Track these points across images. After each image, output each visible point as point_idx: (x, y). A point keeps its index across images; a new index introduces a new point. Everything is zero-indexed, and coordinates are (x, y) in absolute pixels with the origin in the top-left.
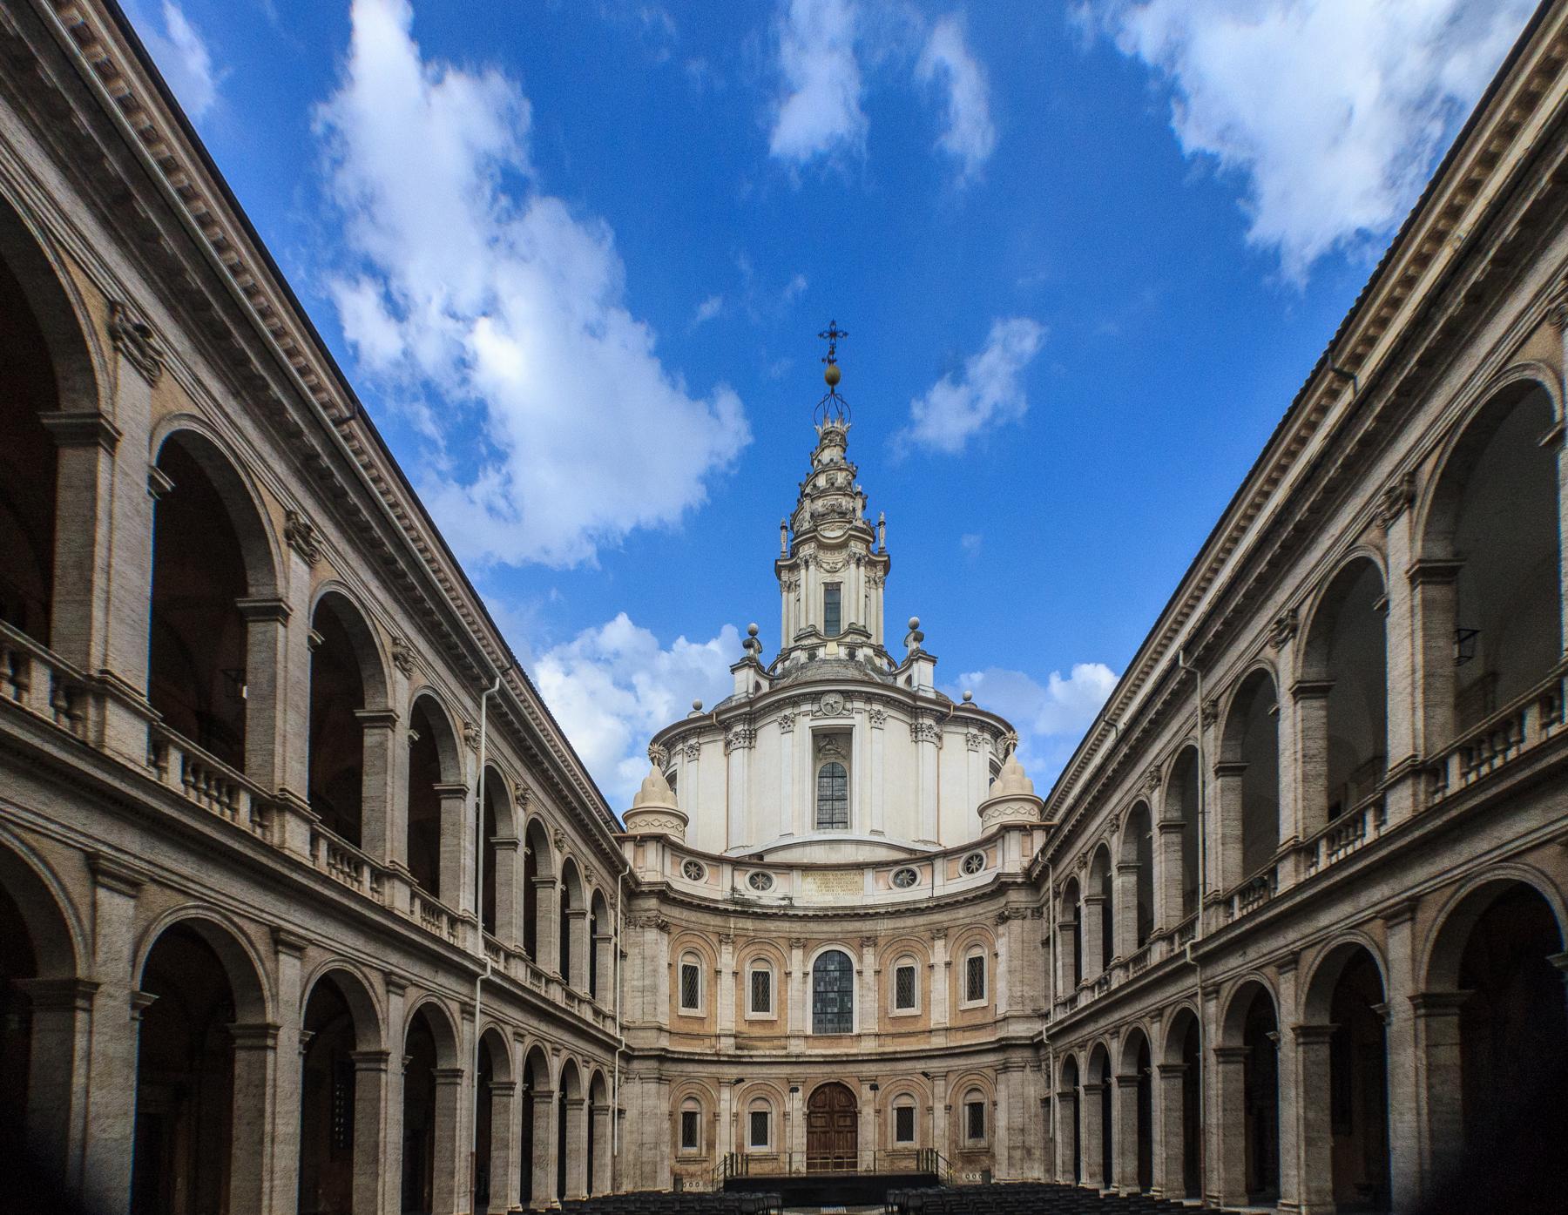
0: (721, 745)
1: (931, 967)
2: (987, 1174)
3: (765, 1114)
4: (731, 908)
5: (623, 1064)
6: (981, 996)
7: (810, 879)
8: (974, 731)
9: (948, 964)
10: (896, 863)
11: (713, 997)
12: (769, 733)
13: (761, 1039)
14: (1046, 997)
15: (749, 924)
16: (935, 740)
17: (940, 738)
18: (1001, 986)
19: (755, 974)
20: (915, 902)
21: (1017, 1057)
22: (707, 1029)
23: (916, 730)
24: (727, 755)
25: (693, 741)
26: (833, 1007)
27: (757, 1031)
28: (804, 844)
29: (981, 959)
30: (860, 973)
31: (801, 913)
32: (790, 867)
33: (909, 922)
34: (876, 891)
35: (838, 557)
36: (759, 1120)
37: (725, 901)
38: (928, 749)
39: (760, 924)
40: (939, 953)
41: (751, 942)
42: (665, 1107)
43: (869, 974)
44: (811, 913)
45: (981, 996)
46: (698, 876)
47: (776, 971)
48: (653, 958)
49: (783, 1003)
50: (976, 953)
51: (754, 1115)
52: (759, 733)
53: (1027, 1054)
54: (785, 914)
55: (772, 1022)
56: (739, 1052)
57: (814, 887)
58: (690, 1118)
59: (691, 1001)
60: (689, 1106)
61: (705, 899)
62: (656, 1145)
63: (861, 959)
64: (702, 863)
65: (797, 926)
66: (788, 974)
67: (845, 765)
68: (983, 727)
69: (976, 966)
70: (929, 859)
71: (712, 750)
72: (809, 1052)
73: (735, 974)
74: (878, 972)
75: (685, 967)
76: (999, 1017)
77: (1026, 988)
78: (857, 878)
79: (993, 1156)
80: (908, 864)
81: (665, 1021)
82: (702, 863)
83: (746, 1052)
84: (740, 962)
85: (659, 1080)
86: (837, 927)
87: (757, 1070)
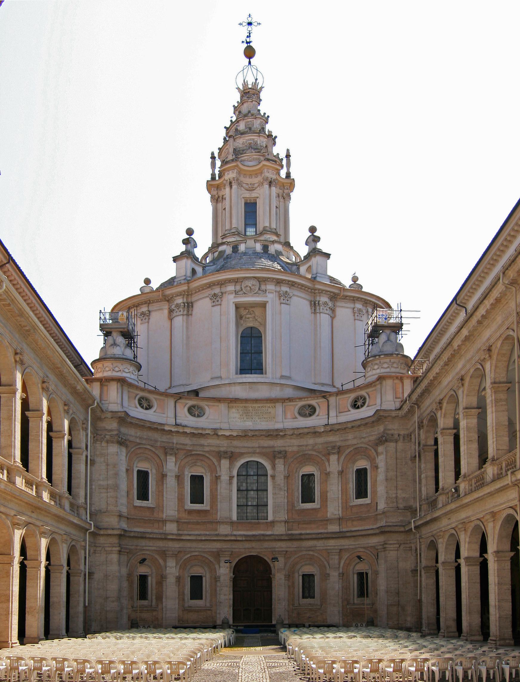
11: (160, 493)
14: (415, 498)
19: (192, 477)
20: (314, 427)
26: (252, 506)
29: (365, 470)
31: (227, 433)
33: (311, 441)
34: (285, 419)
39: (195, 441)
44: (235, 434)
59: (143, 494)
63: (274, 467)
66: (218, 478)
77: (399, 492)
80: (309, 399)
86: (254, 444)
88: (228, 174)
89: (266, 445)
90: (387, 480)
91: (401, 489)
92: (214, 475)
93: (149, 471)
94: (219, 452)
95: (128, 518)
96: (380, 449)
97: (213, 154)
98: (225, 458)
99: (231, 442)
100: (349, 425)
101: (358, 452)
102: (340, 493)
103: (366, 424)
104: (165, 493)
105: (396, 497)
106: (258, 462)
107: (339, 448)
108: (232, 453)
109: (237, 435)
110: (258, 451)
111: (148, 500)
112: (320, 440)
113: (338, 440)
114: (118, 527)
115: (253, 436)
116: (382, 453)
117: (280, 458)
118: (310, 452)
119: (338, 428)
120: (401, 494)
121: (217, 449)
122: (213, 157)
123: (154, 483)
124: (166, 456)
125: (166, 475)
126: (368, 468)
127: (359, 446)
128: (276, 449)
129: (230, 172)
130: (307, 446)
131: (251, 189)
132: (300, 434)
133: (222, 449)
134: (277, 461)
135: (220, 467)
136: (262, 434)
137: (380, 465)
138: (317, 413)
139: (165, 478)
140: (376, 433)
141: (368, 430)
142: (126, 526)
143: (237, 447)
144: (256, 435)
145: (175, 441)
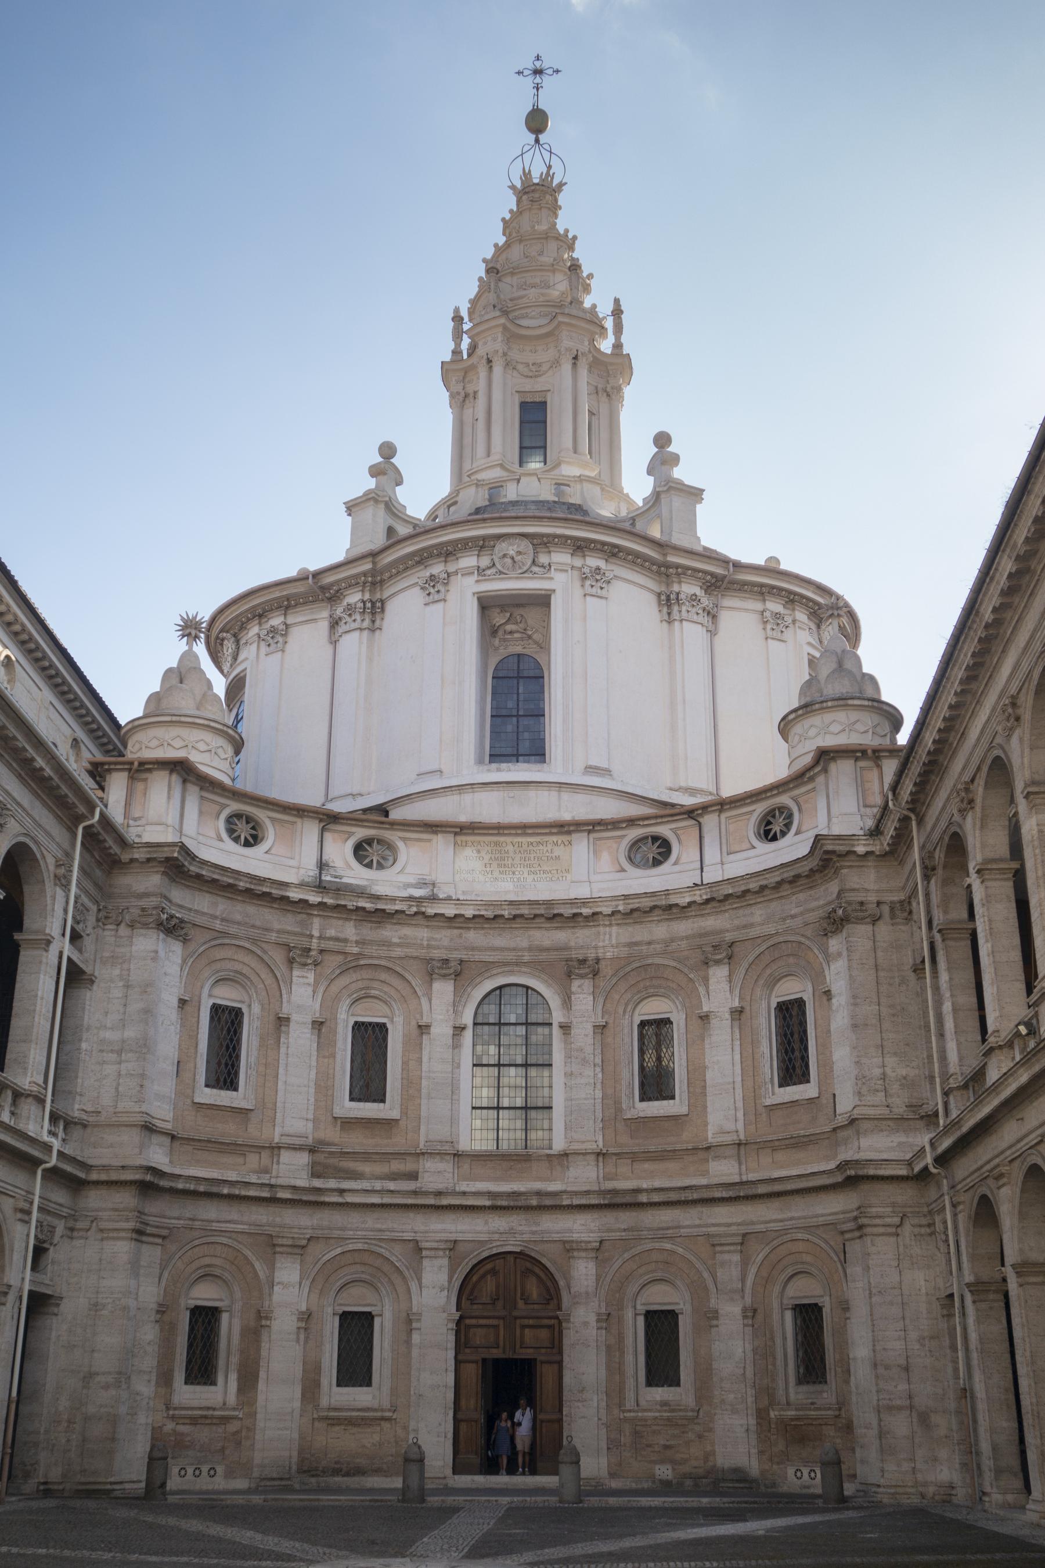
0: (324, 625)
1: (705, 1018)
2: (834, 1466)
3: (369, 1317)
4: (314, 898)
5: (60, 1196)
6: (805, 1078)
7: (469, 852)
8: (774, 606)
9: (738, 1013)
10: (632, 822)
11: (270, 1070)
12: (406, 604)
13: (366, 1157)
15: (349, 930)
16: (705, 619)
17: (714, 617)
18: (842, 1055)
19: (358, 1026)
20: (667, 893)
21: (883, 1202)
22: (254, 1132)
23: (668, 602)
24: (334, 643)
25: (276, 621)
27: (357, 1141)
28: (460, 788)
29: (800, 1003)
30: (565, 1028)
31: (450, 911)
32: (433, 827)
33: (659, 930)
34: (593, 874)
35: (544, 355)
36: (356, 1327)
37: (302, 885)
39: (368, 932)
40: (719, 992)
41: (352, 964)
42: (150, 1293)
43: (583, 1033)
44: (469, 912)
45: (805, 1078)
46: (253, 840)
47: (399, 1020)
48: (147, 987)
49: (411, 1085)
50: (789, 989)
51: (345, 1317)
52: (390, 607)
53: (904, 1195)
54: (418, 912)
55: (387, 1125)
56: (317, 1183)
57: (477, 865)
58: (205, 1319)
59: (225, 1072)
60: (205, 1294)
61: (262, 880)
62: (123, 1377)
63: (567, 1002)
64: (262, 815)
65: (444, 937)
66: (423, 1029)
67: (541, 659)
68: (792, 599)
69: (791, 1018)
70: (692, 813)
71: (308, 634)
72: (463, 1187)
73: (318, 1025)
74: (601, 1029)
75: (216, 1009)
76: (841, 1120)
78: (558, 851)
79: (849, 1428)
81: (163, 1113)
82: (262, 815)
83: (332, 1184)
84: (330, 1004)
85: (139, 1234)
86: (520, 939)
87: (353, 1220)
88: (485, 343)
89: (547, 943)
90: (855, 1026)
91: (895, 1054)
92: (414, 1023)
93: (245, 1010)
94: (429, 961)
95: (173, 1137)
96: (835, 944)
97: (457, 310)
98: (444, 976)
99: (460, 936)
100: (753, 885)
101: (781, 954)
102: (738, 1068)
103: (797, 877)
104: (281, 1071)
105: (884, 1074)
106: (527, 988)
107: (731, 945)
108: (461, 962)
109: (475, 916)
110: (526, 959)
111: (236, 1089)
112: (683, 927)
114: (139, 1162)
115: (515, 917)
116: (839, 954)
117: (582, 977)
118: (658, 961)
120: (896, 1068)
121: (422, 953)
122: (457, 319)
123: (255, 1043)
124: (291, 969)
125: (288, 1019)
126: (807, 997)
127: (781, 939)
128: (574, 955)
129: (489, 339)
130: (649, 943)
131: (536, 371)
132: (632, 911)
133: (437, 954)
134: (575, 984)
135: (430, 1000)
136: (538, 912)
137: (834, 990)
139: (283, 1028)
140: (822, 902)
141: (802, 896)
142: (167, 1160)
143: (473, 949)
144: (521, 916)
145: (316, 933)
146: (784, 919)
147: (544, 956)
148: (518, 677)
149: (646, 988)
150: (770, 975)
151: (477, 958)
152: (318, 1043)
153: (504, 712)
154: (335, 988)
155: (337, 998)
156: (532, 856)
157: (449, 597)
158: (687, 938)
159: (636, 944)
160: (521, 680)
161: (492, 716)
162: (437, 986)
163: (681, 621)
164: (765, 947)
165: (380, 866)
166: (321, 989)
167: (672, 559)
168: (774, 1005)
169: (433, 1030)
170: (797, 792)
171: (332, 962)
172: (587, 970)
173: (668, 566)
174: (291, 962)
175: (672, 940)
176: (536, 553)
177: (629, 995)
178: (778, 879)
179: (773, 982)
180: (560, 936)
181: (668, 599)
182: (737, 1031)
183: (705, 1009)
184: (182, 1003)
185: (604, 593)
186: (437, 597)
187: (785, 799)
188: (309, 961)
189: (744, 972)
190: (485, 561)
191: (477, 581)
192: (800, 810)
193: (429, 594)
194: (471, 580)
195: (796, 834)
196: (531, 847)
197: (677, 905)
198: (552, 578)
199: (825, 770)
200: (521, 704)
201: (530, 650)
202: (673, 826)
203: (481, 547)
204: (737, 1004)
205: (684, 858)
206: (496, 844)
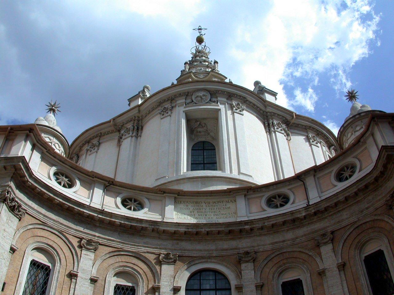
1: (322, 274)
9: (342, 267)
25: (95, 141)
29: (380, 253)
38: (281, 137)
40: (329, 258)
50: (371, 249)
63: (239, 275)
73: (93, 281)
75: (34, 264)
89: (225, 246)
100: (341, 198)
103: (366, 187)
106: (216, 272)
107: (332, 233)
109: (185, 233)
110: (214, 255)
113: (328, 224)
117: (247, 262)
119: (326, 206)
125: (76, 276)
127: (361, 222)
130: (284, 241)
132: (273, 225)
134: (243, 266)
138: (291, 201)
141: (370, 198)
143: (185, 250)
146: (362, 211)
147: (224, 253)
148: (204, 150)
149: (284, 264)
150: (358, 243)
151: (187, 254)
152: (94, 292)
153: (197, 162)
154: (105, 264)
155: (107, 269)
156: (215, 208)
157: (173, 115)
158: (305, 235)
159: (276, 243)
160: (205, 151)
161: (192, 164)
162: (164, 267)
163: (275, 132)
164: (352, 229)
165: (134, 210)
166: (98, 263)
167: (269, 109)
168: (364, 258)
169: (161, 290)
170: (355, 154)
171: (103, 251)
172: (250, 258)
173: (267, 113)
174: (80, 247)
175: (297, 238)
176: (211, 97)
177: (274, 269)
178: (356, 190)
179: (361, 247)
180: (234, 244)
181: (269, 125)
182: (343, 276)
183: (321, 267)
184: (13, 250)
185: (241, 113)
186: (167, 115)
187: (350, 160)
188: (91, 248)
189: (341, 244)
190: (189, 101)
191: (185, 107)
192: (359, 160)
193: (163, 115)
194: (183, 107)
195: (359, 171)
196: (215, 204)
197: (298, 218)
198: (218, 106)
199: (373, 135)
200: (205, 159)
201: (209, 139)
202: (290, 187)
203: (187, 96)
204: (340, 261)
205: (297, 201)
206: (196, 203)
